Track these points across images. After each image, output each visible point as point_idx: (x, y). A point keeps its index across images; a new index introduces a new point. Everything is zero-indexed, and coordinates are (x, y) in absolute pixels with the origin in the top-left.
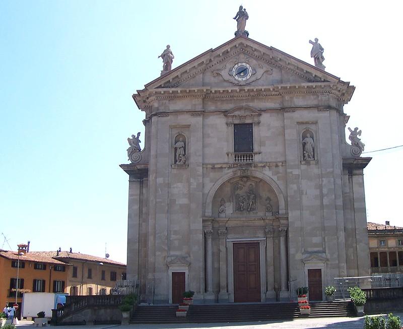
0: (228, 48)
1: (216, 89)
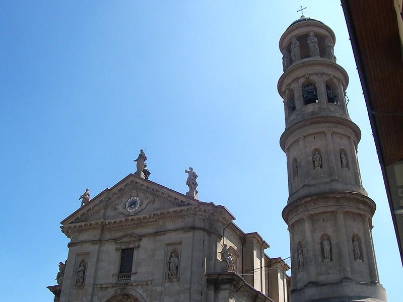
0: (122, 186)
1: (109, 221)
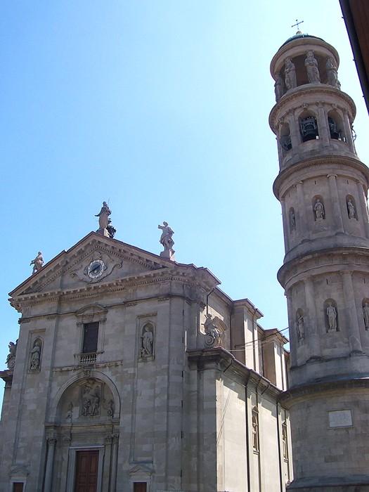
0: (82, 247)
1: (68, 290)
